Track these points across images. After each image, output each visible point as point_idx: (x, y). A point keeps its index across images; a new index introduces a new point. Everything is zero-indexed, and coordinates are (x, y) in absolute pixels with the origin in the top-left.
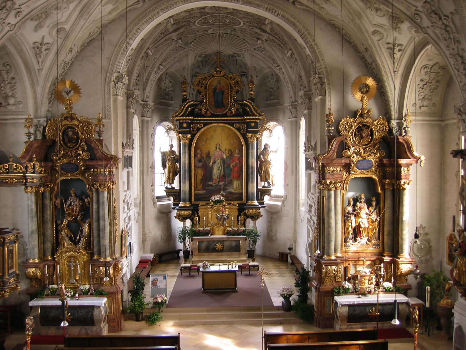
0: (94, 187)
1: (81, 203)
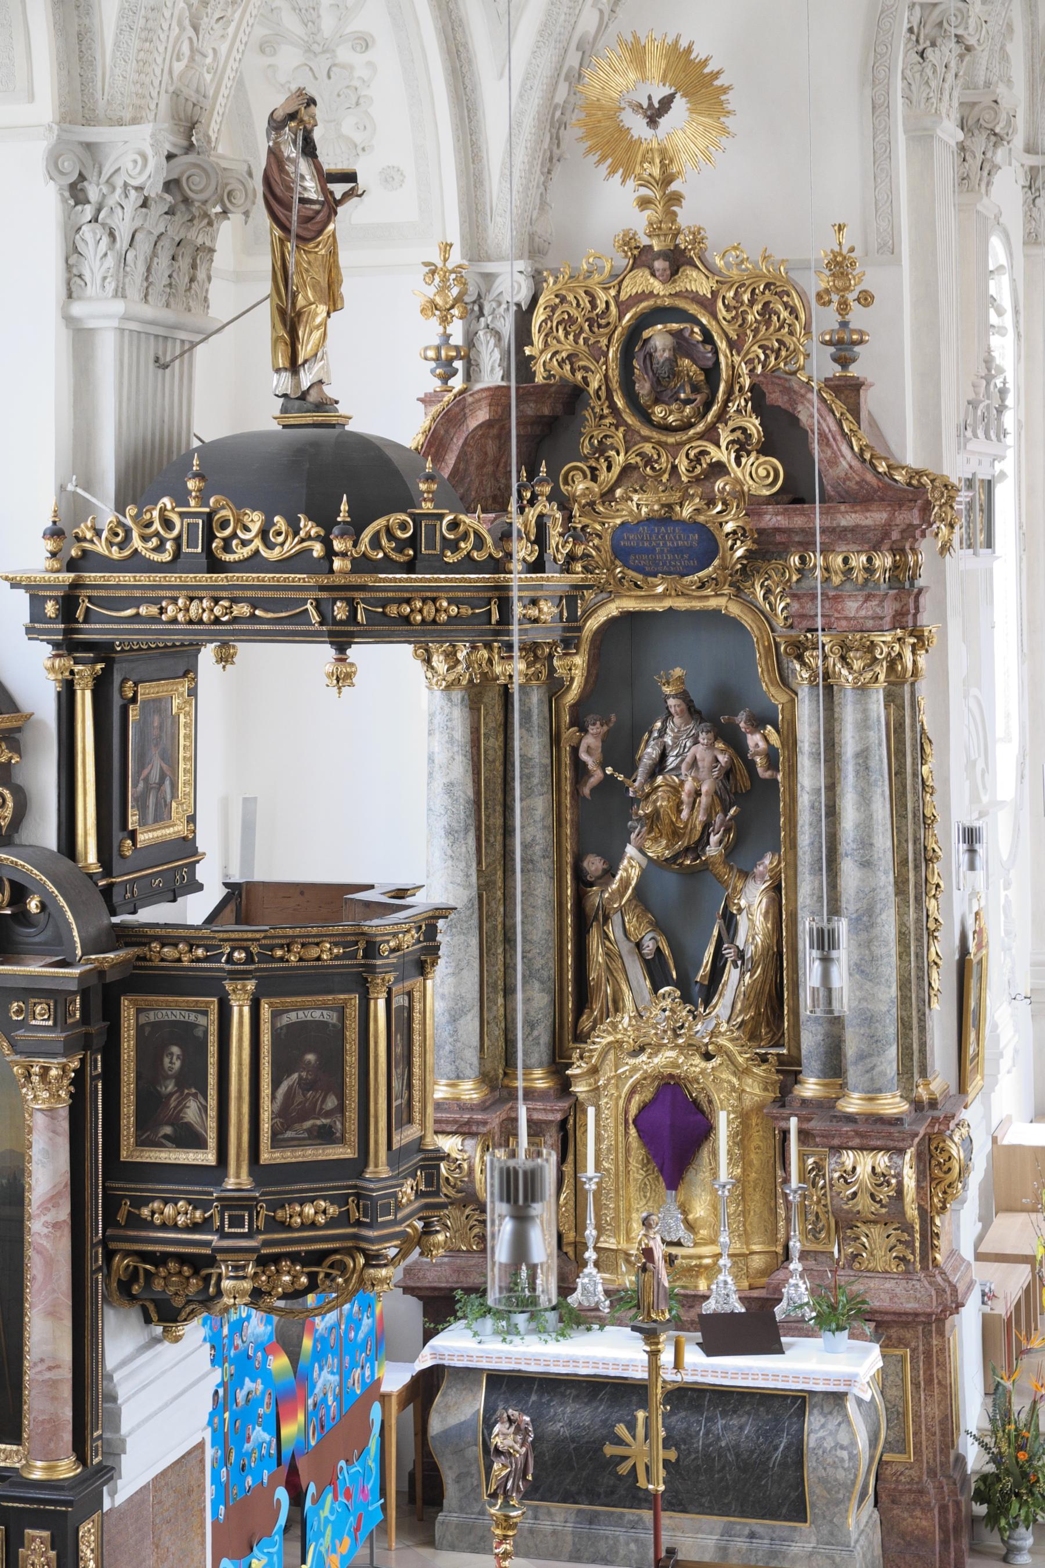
0: (803, 664)
1: (722, 751)
